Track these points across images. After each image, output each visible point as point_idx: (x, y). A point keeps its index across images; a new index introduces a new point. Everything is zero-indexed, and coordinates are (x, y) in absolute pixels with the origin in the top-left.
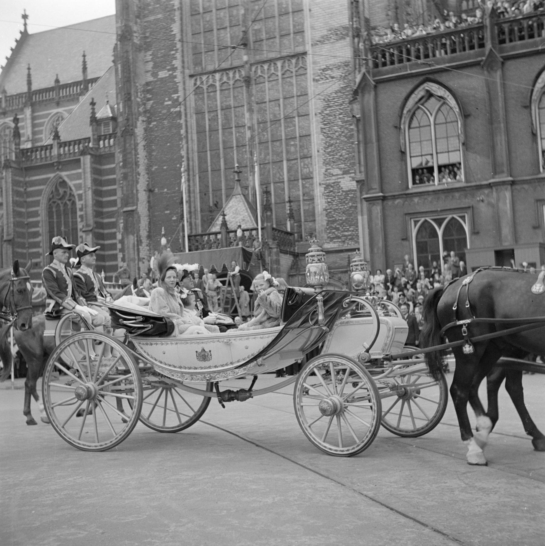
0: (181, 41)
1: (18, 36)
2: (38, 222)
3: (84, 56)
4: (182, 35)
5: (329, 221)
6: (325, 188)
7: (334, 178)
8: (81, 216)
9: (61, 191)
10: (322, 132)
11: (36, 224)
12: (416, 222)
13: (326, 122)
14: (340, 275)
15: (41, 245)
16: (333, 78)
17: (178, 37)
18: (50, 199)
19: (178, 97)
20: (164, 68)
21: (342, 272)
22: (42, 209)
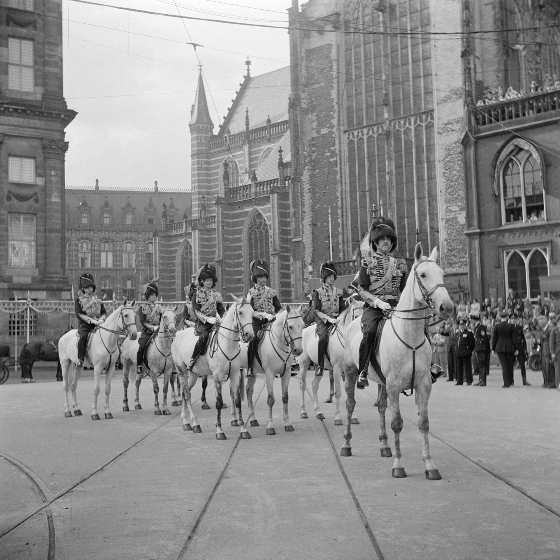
0: (338, 103)
1: (242, 80)
2: (241, 246)
4: (338, 99)
6: (446, 223)
7: (453, 214)
9: (258, 221)
10: (444, 175)
11: (239, 248)
12: (508, 253)
13: (448, 168)
16: (453, 131)
17: (335, 101)
18: (250, 228)
20: (325, 126)
22: (244, 236)
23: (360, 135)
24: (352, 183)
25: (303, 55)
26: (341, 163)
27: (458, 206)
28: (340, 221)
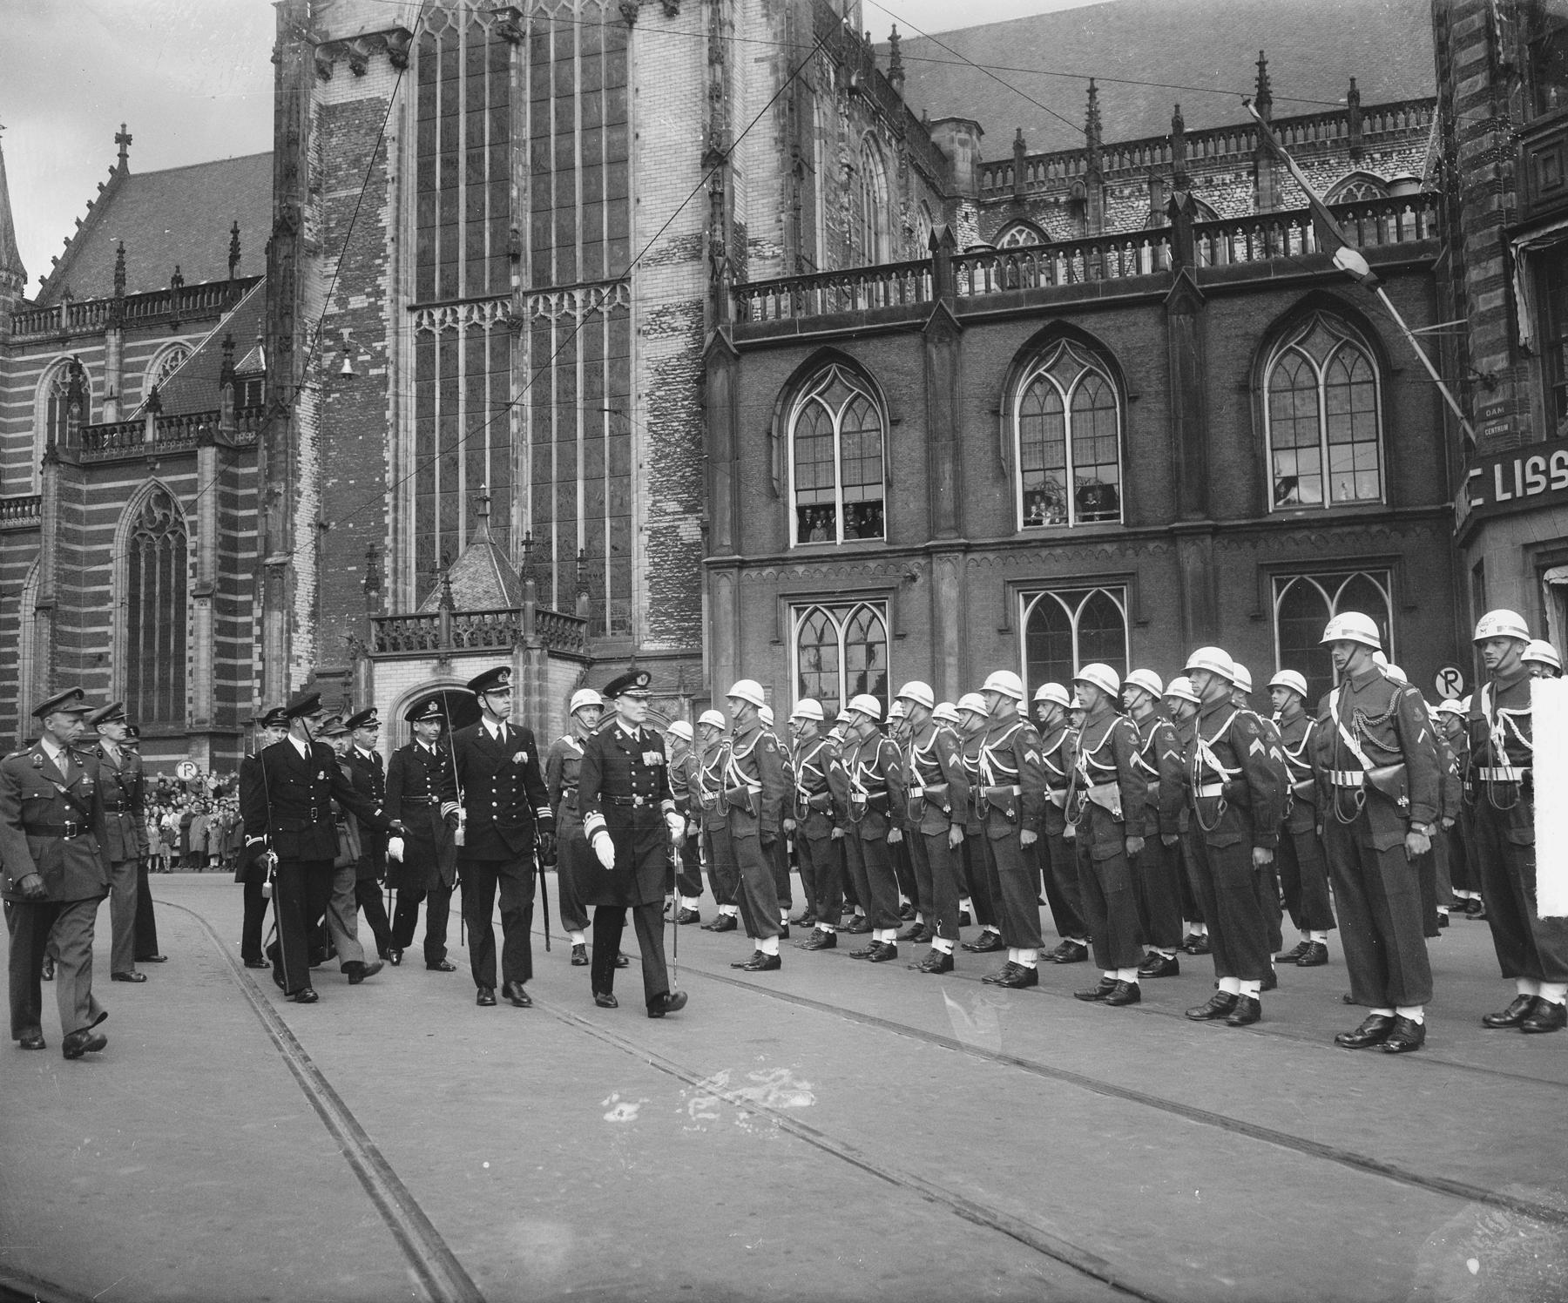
0: (396, 239)
2: (109, 573)
3: (235, 232)
4: (397, 229)
5: (654, 600)
7: (668, 518)
8: (193, 566)
13: (657, 411)
14: (663, 703)
15: (112, 618)
16: (674, 330)
17: (390, 233)
18: (135, 528)
19: (385, 347)
20: (360, 291)
21: (667, 698)
23: (449, 319)
24: (424, 434)
25: (312, 116)
26: (397, 382)
27: (680, 502)
28: (388, 519)
